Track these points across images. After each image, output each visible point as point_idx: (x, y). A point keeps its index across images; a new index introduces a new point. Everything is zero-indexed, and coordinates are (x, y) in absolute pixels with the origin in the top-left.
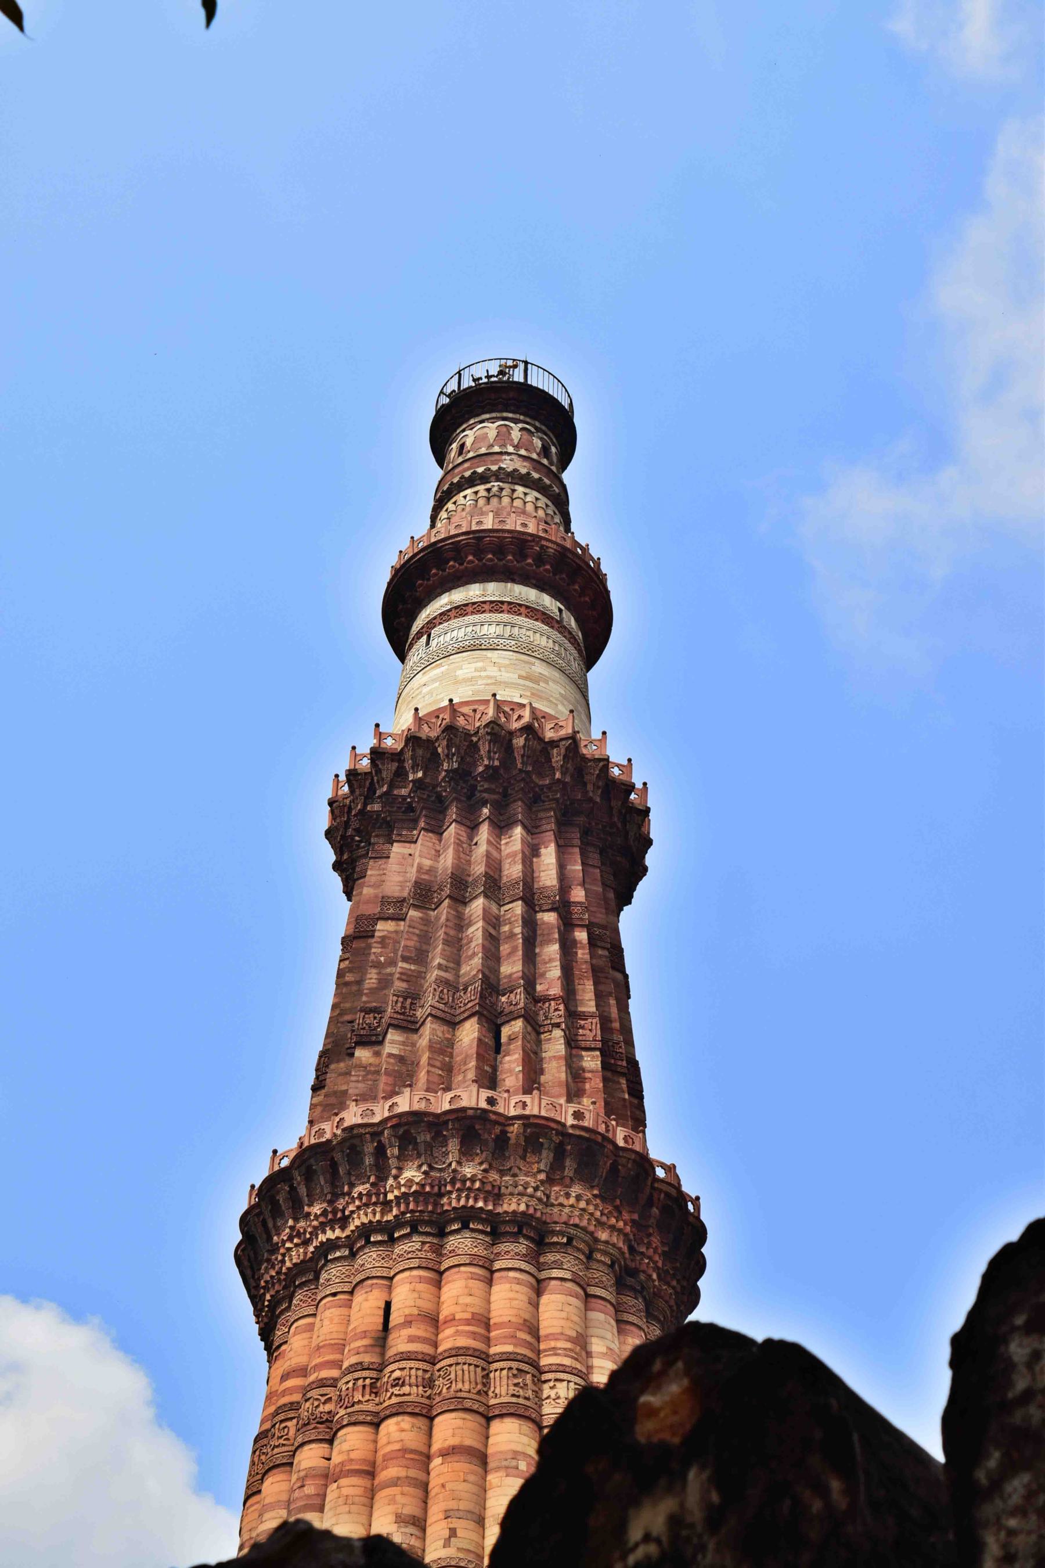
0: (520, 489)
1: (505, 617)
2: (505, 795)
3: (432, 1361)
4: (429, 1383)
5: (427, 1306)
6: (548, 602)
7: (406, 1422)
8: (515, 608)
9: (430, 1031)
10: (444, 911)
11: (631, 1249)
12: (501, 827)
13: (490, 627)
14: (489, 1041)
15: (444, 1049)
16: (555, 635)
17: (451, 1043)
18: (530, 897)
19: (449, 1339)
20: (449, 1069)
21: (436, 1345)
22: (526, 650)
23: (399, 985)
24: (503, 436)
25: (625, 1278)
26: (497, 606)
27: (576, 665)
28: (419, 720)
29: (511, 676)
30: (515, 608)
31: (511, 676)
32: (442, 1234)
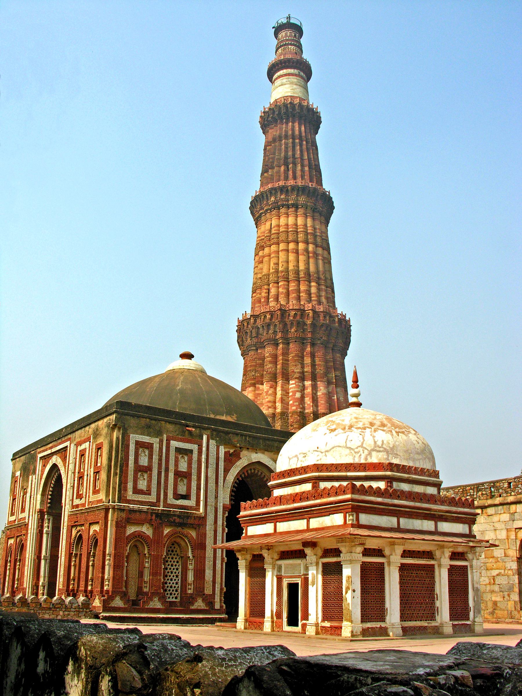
0: (290, 46)
1: (287, 77)
2: (288, 116)
3: (278, 234)
4: (278, 238)
5: (277, 223)
6: (296, 71)
7: (274, 246)
8: (289, 75)
9: (276, 169)
10: (277, 144)
11: (315, 205)
12: (287, 123)
13: (284, 80)
14: (287, 169)
15: (278, 172)
16: (298, 78)
17: (280, 170)
18: (293, 137)
19: (282, 229)
20: (280, 176)
21: (279, 230)
22: (292, 83)
23: (271, 160)
24: (286, 34)
25: (314, 210)
26: (285, 75)
27: (302, 83)
28: (271, 105)
29: (289, 90)
30: (289, 75)
31: (289, 90)
32: (279, 209)
